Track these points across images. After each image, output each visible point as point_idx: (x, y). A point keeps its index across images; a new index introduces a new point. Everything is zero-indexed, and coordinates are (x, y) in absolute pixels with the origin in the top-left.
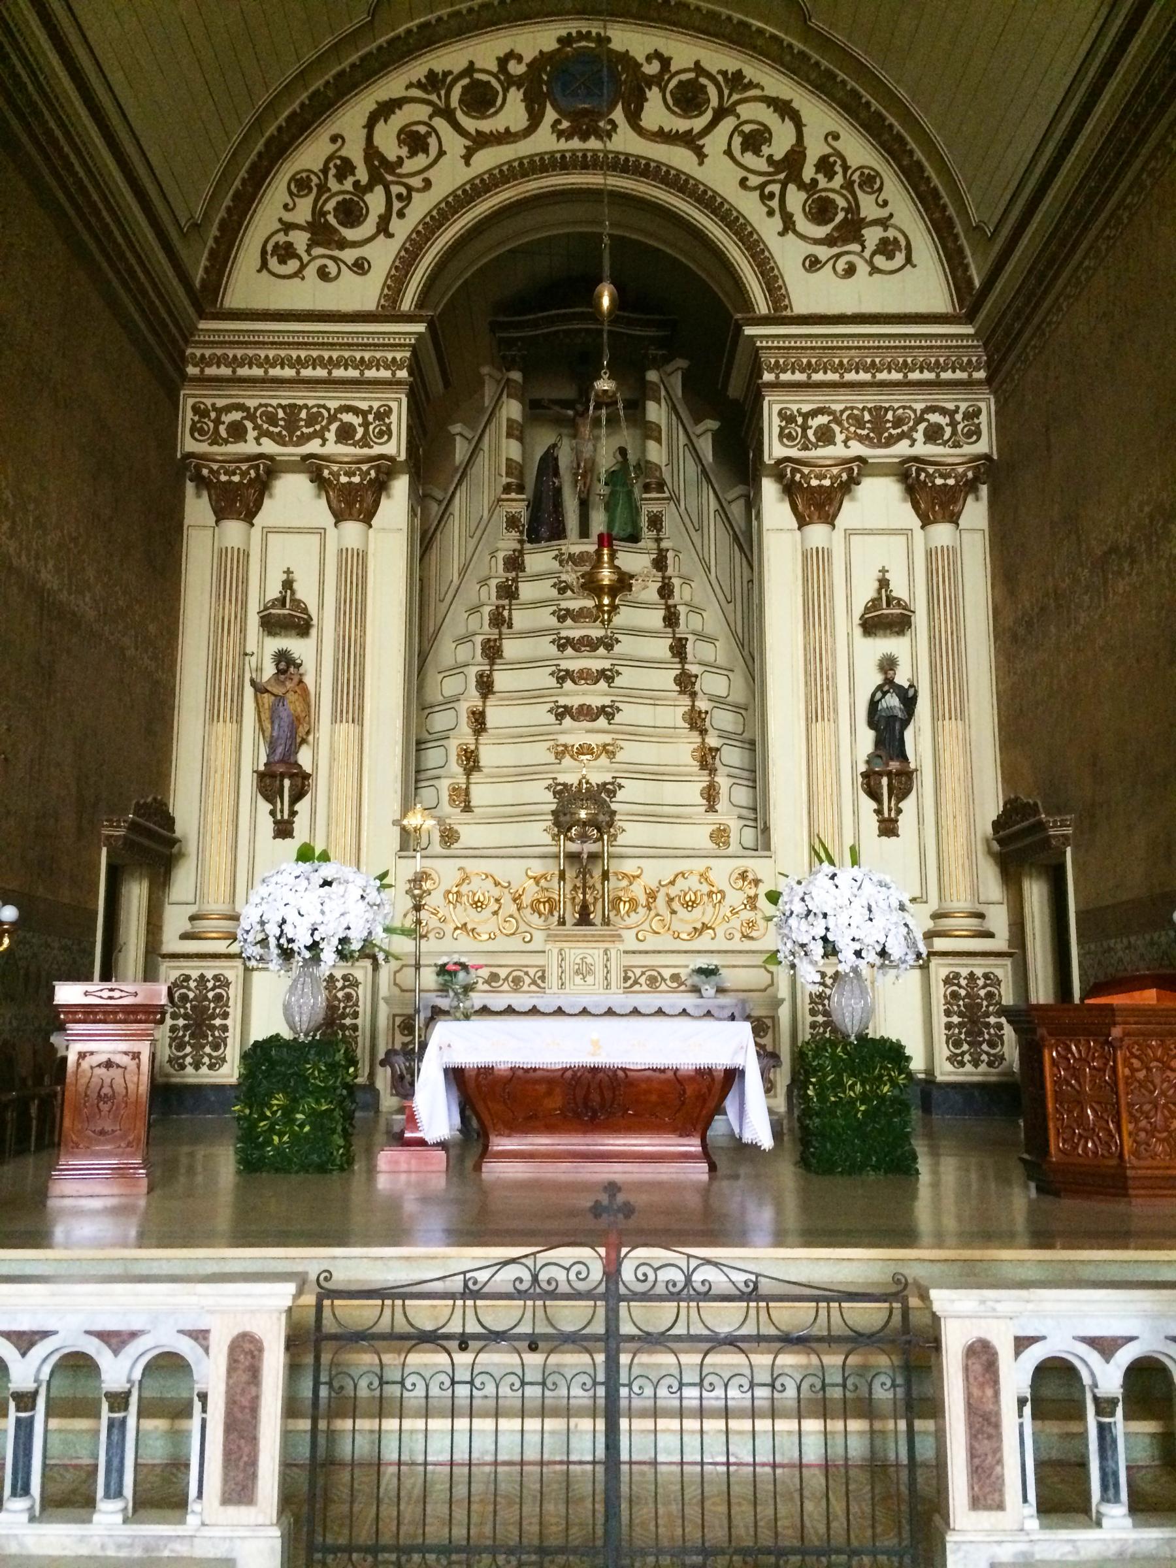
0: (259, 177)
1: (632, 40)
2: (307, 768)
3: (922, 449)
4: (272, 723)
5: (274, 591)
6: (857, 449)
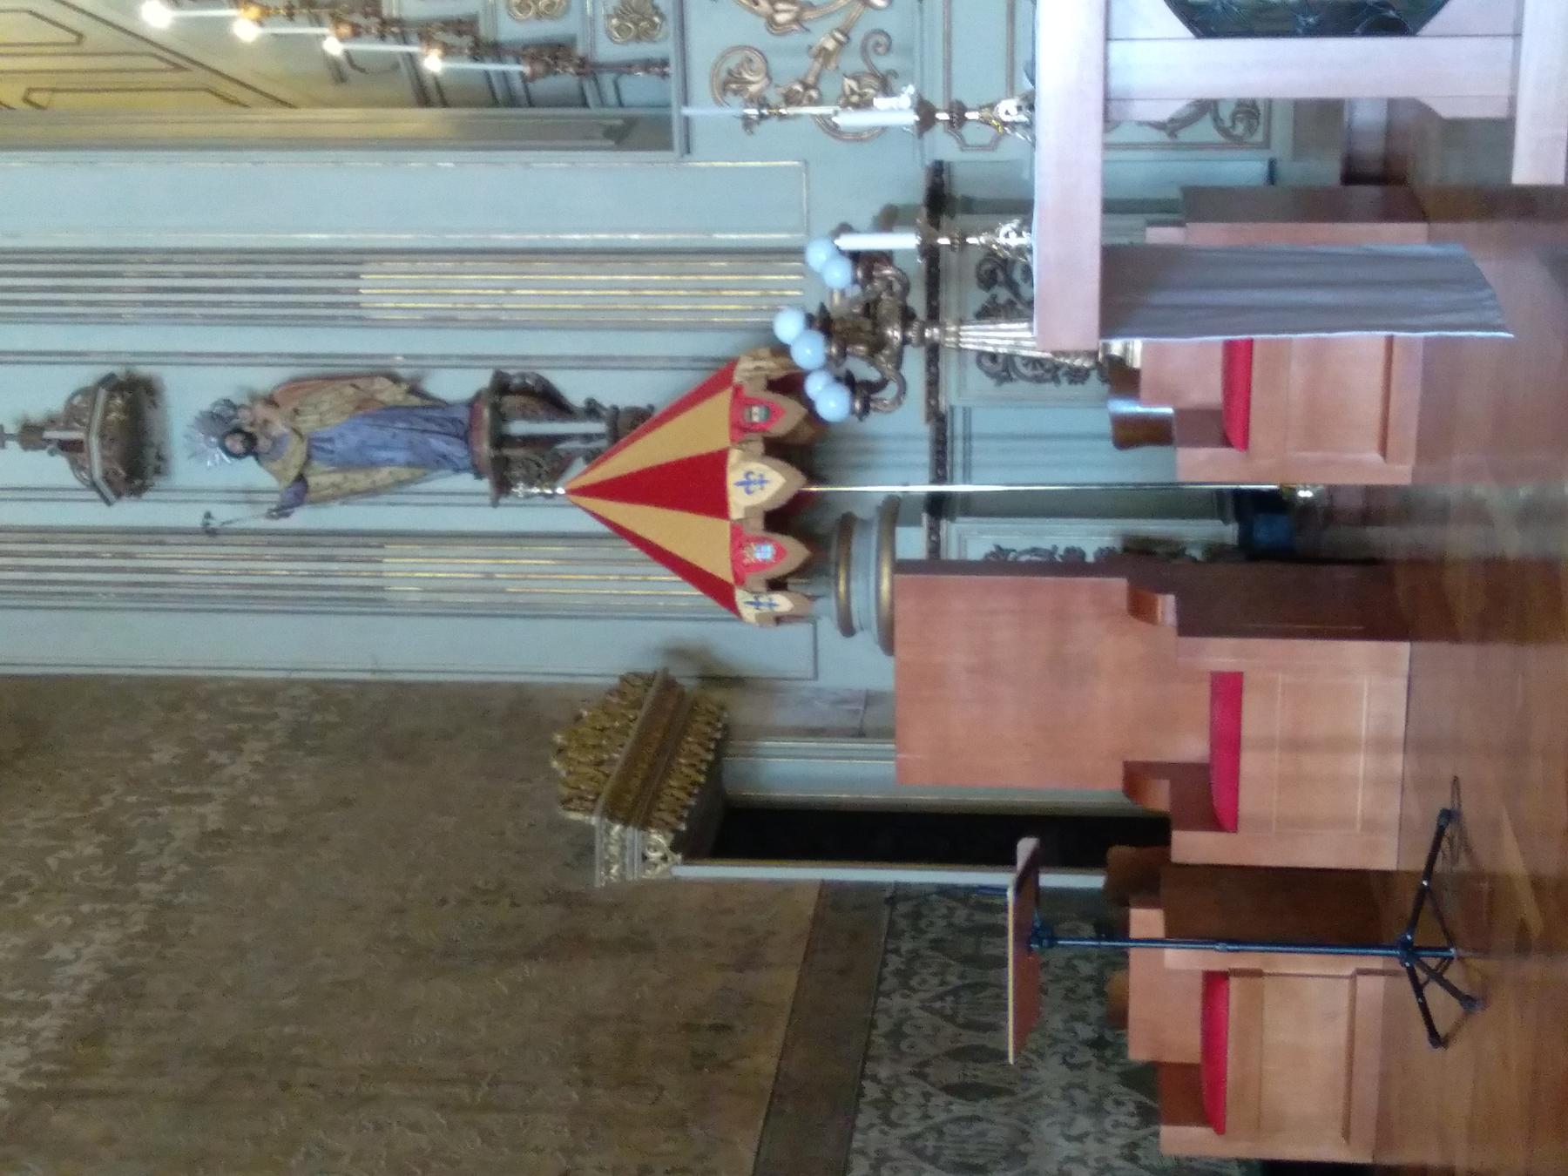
2: (481, 380)
4: (374, 464)
5: (54, 469)
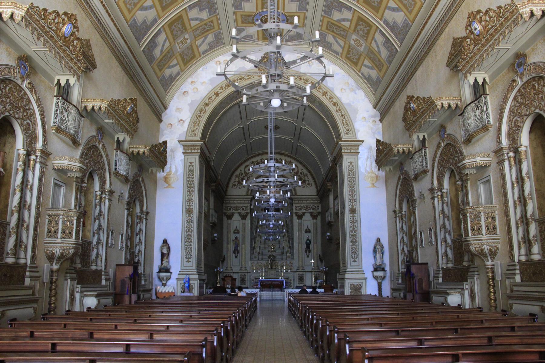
3: (311, 211)
5: (234, 228)
6: (304, 211)
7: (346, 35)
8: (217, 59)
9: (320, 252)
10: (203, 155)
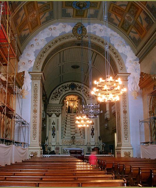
0: (51, 93)
1: (76, 83)
7: (123, 15)
8: (49, 27)
9: (99, 135)
10: (42, 80)
